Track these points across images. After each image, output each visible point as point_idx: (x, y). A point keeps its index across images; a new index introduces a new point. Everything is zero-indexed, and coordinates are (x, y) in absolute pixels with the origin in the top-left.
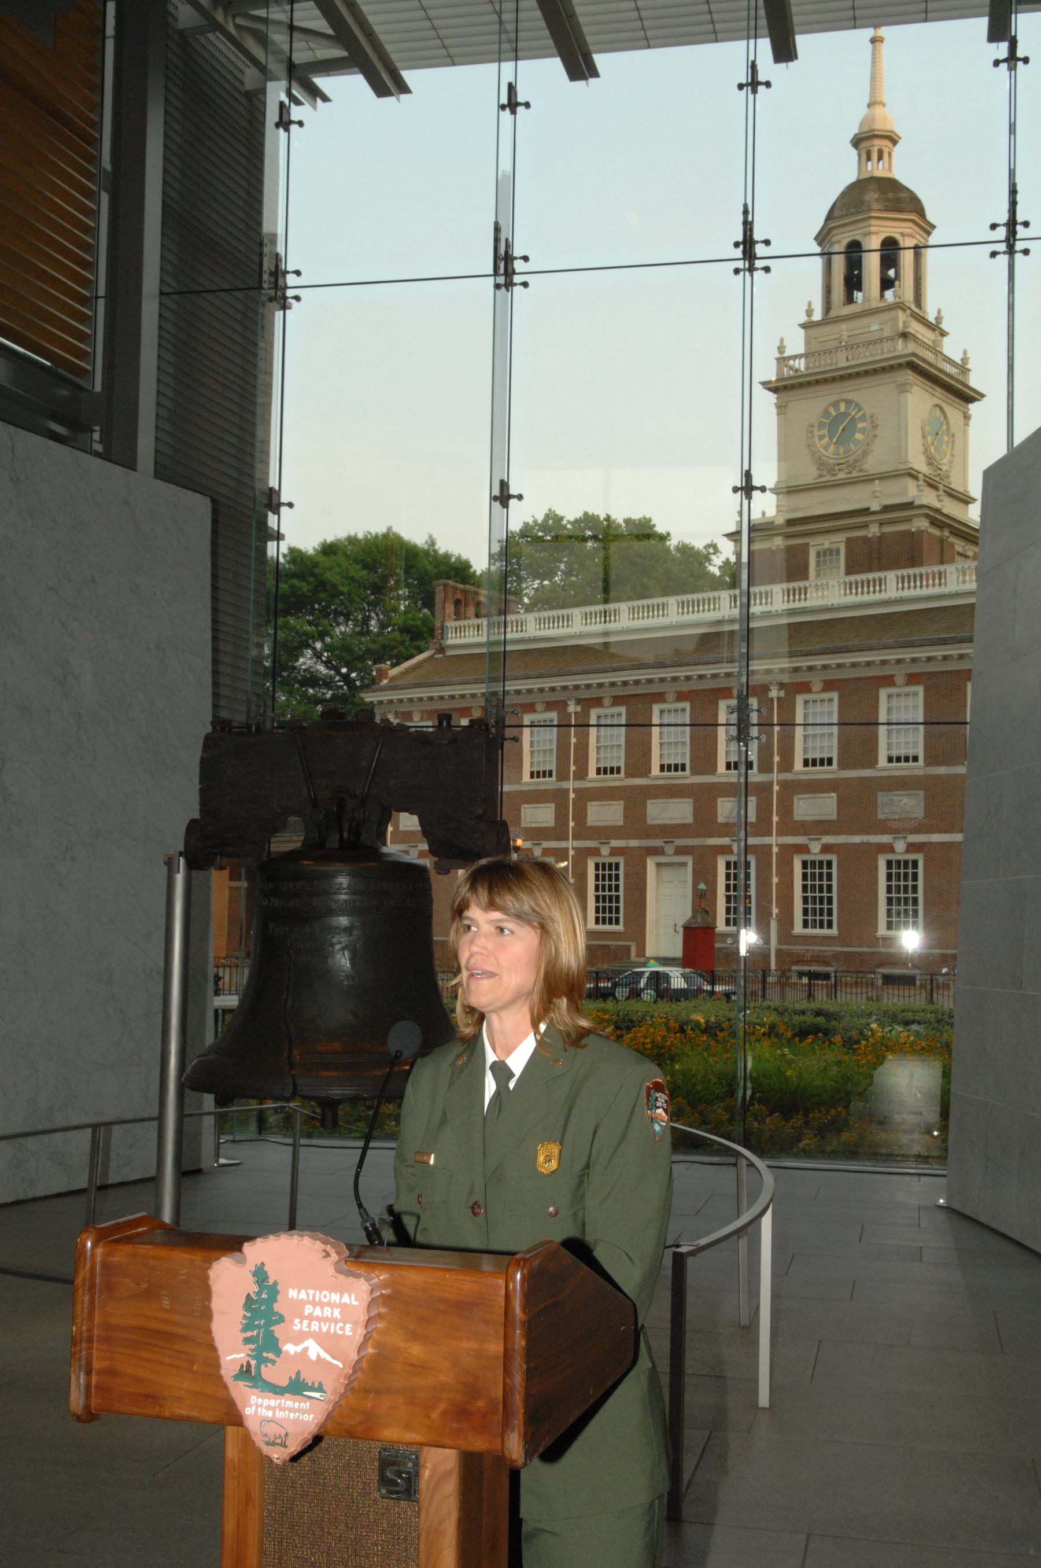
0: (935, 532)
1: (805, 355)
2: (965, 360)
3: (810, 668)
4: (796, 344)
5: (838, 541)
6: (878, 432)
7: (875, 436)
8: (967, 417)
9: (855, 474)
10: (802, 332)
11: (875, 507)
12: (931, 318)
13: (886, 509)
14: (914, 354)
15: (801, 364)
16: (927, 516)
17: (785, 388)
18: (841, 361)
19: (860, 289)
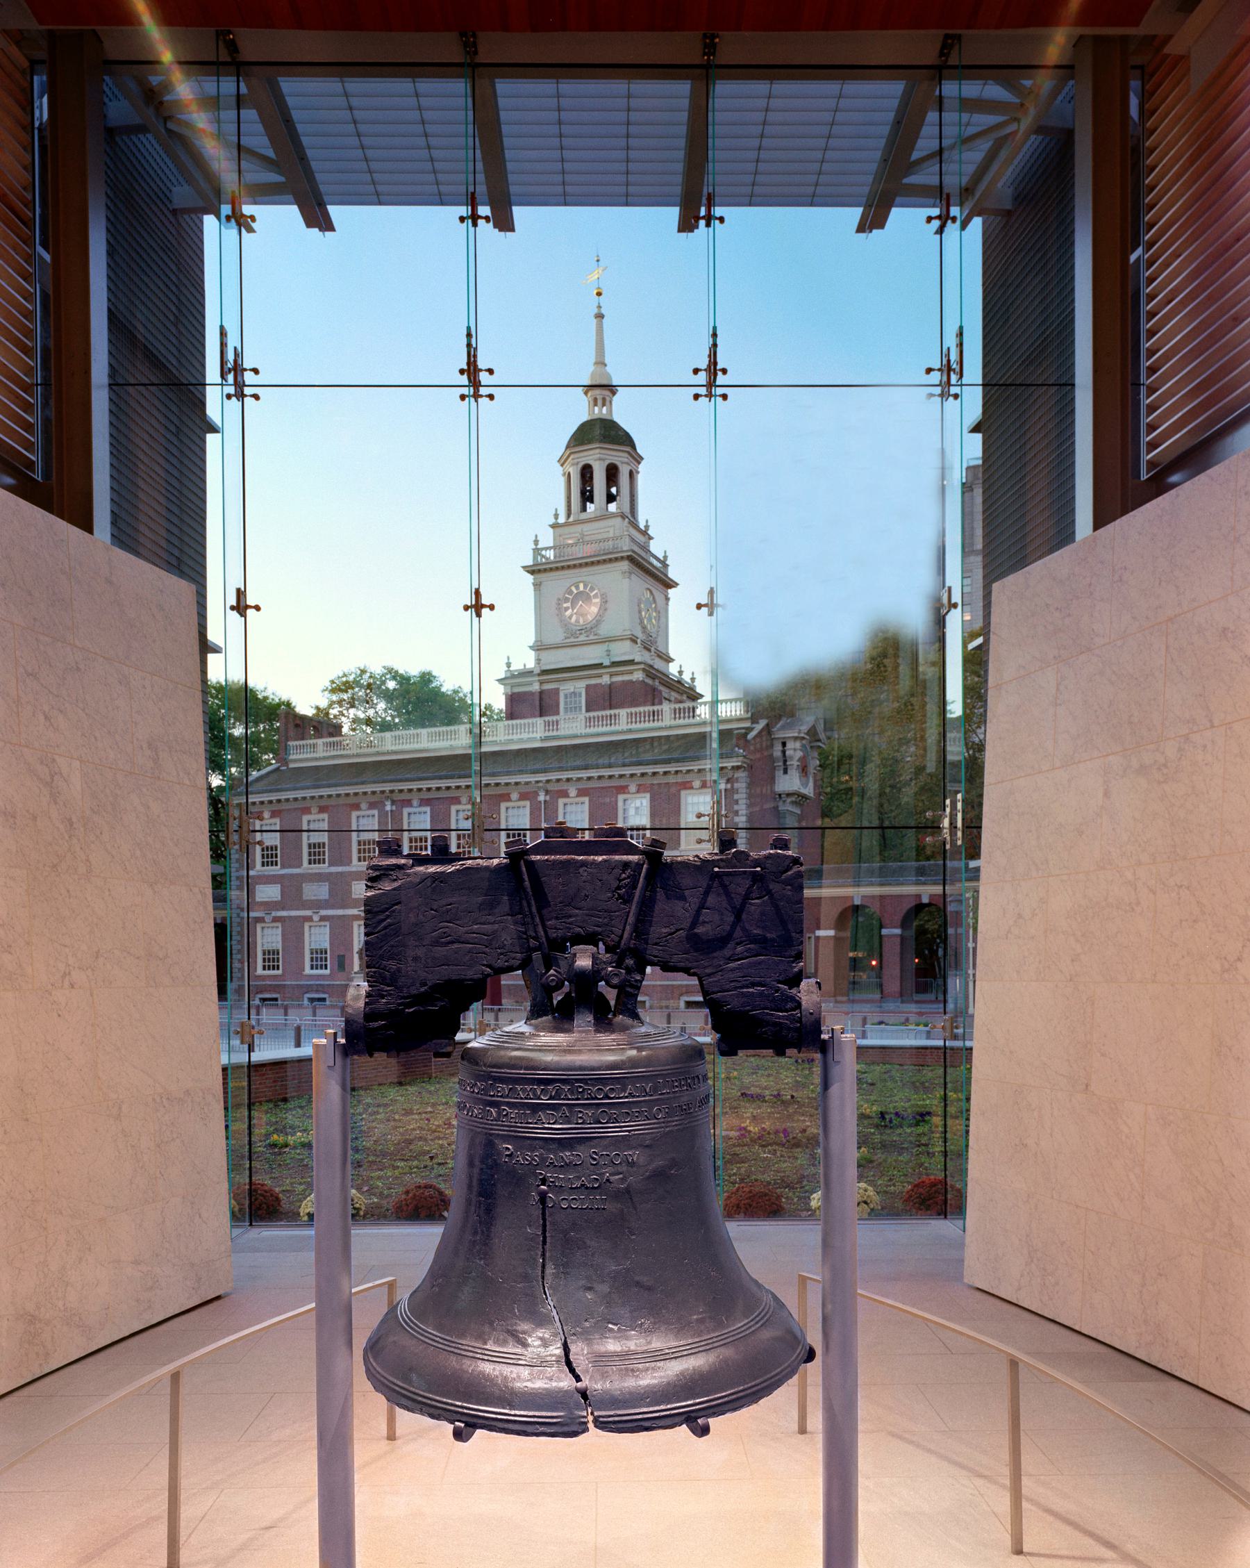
0: (649, 681)
1: (554, 548)
2: (665, 557)
3: (568, 780)
4: (547, 539)
5: (580, 686)
6: (607, 605)
7: (606, 610)
8: (667, 599)
9: (592, 637)
10: (551, 530)
11: (607, 663)
12: (642, 526)
13: (614, 664)
14: (633, 551)
15: (550, 554)
16: (644, 670)
17: (539, 571)
18: (581, 552)
19: (592, 502)
